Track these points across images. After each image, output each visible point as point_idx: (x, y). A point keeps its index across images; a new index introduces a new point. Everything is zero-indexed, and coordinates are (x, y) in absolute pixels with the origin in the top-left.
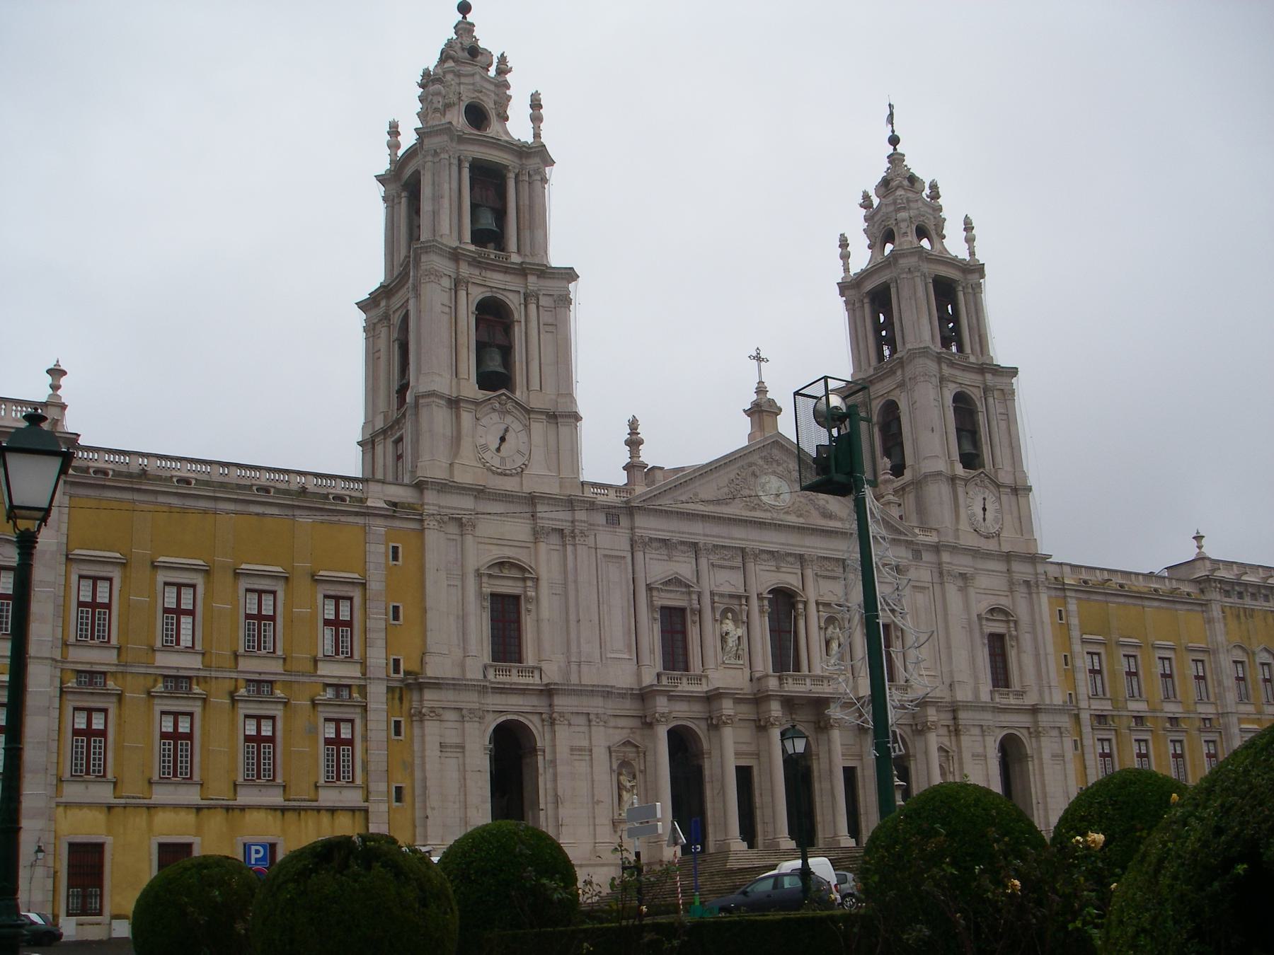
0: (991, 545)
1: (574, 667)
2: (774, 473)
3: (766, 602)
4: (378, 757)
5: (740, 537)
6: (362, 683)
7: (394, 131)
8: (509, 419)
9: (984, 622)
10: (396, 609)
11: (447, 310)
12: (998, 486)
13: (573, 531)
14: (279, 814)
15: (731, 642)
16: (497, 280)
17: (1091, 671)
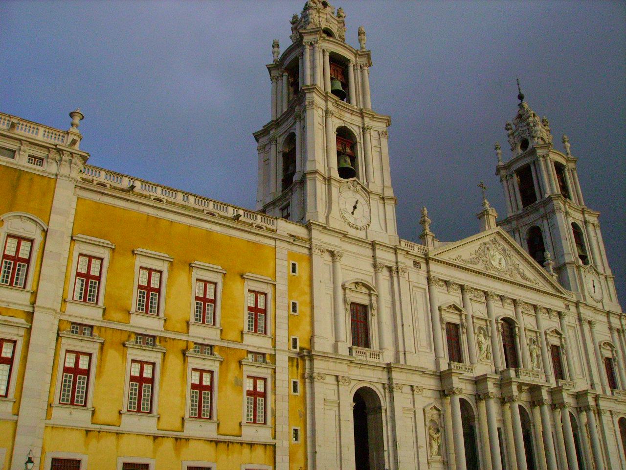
1: (401, 355)
3: (500, 325)
6: (273, 352)
7: (276, 45)
11: (321, 127)
13: (397, 268)
14: (214, 444)
15: (484, 347)
16: (347, 116)
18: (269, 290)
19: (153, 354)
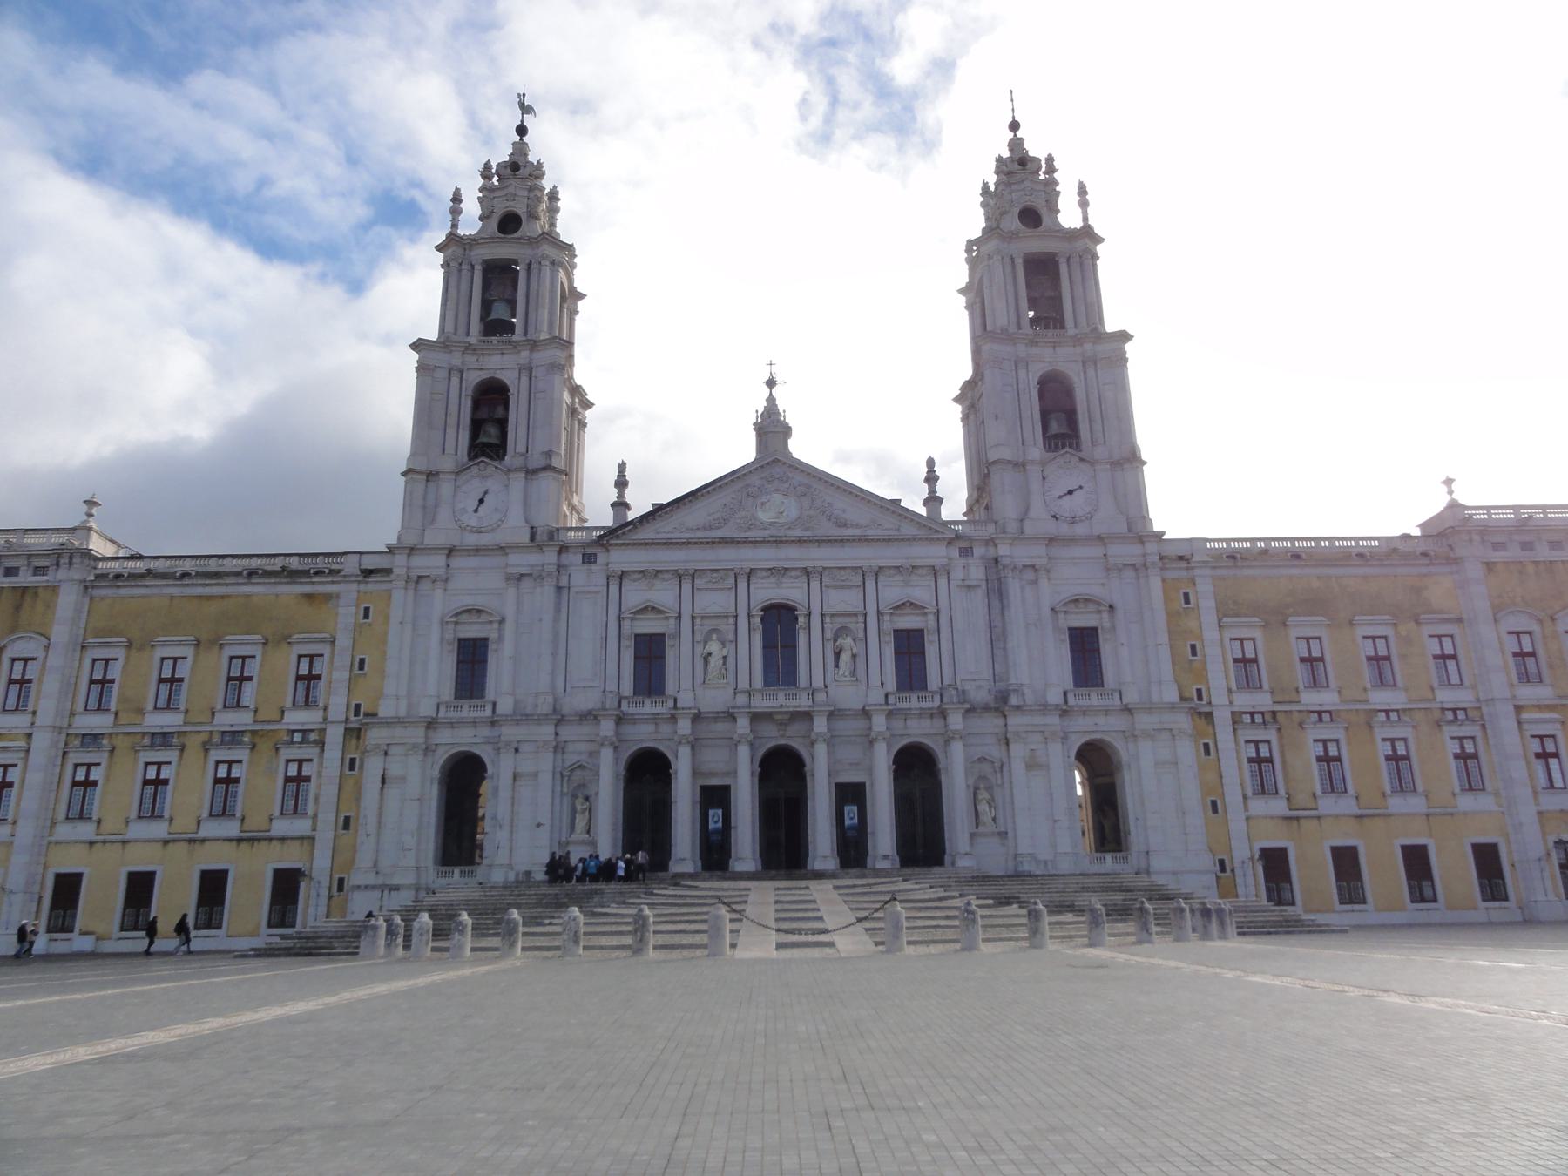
0: (1080, 530)
2: (777, 491)
4: (329, 791)
8: (489, 484)
9: (1061, 616)
10: (362, 661)
12: (1093, 463)
17: (1236, 661)
18: (325, 649)
19: (168, 753)
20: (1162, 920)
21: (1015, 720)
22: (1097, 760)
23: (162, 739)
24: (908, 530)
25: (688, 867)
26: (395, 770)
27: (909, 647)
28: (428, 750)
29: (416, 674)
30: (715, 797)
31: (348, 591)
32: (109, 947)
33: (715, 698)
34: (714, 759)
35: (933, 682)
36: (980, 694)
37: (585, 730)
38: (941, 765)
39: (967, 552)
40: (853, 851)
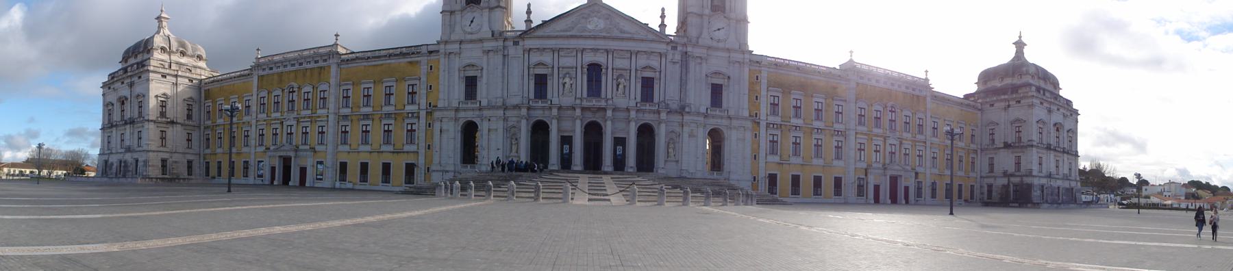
4: (422, 135)
5: (574, 43)
20: (732, 198)
21: (686, 118)
22: (716, 136)
23: (366, 116)
24: (651, 37)
25: (555, 168)
26: (444, 127)
27: (648, 84)
28: (456, 120)
29: (451, 91)
30: (566, 140)
31: (424, 60)
32: (357, 187)
33: (567, 101)
34: (567, 125)
35: (656, 99)
36: (674, 106)
37: (516, 112)
38: (656, 131)
39: (674, 48)
40: (619, 164)
